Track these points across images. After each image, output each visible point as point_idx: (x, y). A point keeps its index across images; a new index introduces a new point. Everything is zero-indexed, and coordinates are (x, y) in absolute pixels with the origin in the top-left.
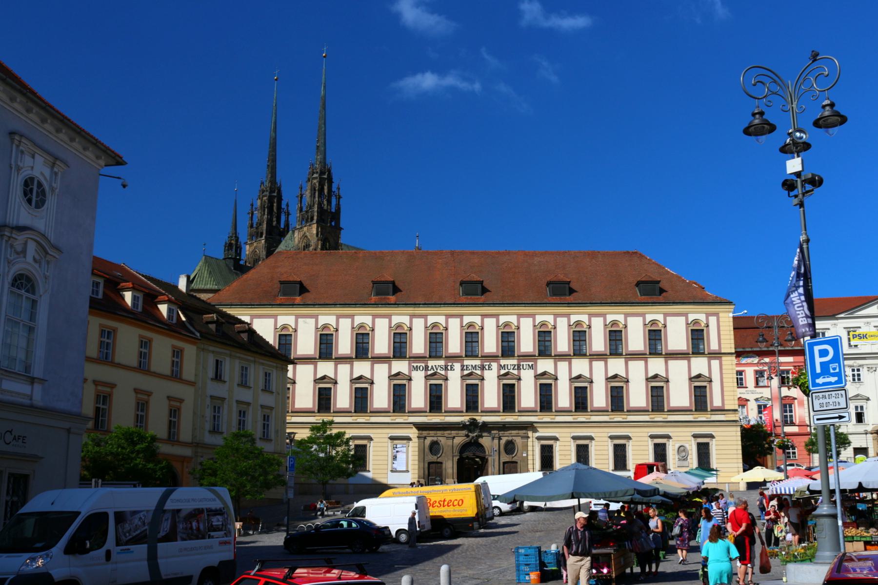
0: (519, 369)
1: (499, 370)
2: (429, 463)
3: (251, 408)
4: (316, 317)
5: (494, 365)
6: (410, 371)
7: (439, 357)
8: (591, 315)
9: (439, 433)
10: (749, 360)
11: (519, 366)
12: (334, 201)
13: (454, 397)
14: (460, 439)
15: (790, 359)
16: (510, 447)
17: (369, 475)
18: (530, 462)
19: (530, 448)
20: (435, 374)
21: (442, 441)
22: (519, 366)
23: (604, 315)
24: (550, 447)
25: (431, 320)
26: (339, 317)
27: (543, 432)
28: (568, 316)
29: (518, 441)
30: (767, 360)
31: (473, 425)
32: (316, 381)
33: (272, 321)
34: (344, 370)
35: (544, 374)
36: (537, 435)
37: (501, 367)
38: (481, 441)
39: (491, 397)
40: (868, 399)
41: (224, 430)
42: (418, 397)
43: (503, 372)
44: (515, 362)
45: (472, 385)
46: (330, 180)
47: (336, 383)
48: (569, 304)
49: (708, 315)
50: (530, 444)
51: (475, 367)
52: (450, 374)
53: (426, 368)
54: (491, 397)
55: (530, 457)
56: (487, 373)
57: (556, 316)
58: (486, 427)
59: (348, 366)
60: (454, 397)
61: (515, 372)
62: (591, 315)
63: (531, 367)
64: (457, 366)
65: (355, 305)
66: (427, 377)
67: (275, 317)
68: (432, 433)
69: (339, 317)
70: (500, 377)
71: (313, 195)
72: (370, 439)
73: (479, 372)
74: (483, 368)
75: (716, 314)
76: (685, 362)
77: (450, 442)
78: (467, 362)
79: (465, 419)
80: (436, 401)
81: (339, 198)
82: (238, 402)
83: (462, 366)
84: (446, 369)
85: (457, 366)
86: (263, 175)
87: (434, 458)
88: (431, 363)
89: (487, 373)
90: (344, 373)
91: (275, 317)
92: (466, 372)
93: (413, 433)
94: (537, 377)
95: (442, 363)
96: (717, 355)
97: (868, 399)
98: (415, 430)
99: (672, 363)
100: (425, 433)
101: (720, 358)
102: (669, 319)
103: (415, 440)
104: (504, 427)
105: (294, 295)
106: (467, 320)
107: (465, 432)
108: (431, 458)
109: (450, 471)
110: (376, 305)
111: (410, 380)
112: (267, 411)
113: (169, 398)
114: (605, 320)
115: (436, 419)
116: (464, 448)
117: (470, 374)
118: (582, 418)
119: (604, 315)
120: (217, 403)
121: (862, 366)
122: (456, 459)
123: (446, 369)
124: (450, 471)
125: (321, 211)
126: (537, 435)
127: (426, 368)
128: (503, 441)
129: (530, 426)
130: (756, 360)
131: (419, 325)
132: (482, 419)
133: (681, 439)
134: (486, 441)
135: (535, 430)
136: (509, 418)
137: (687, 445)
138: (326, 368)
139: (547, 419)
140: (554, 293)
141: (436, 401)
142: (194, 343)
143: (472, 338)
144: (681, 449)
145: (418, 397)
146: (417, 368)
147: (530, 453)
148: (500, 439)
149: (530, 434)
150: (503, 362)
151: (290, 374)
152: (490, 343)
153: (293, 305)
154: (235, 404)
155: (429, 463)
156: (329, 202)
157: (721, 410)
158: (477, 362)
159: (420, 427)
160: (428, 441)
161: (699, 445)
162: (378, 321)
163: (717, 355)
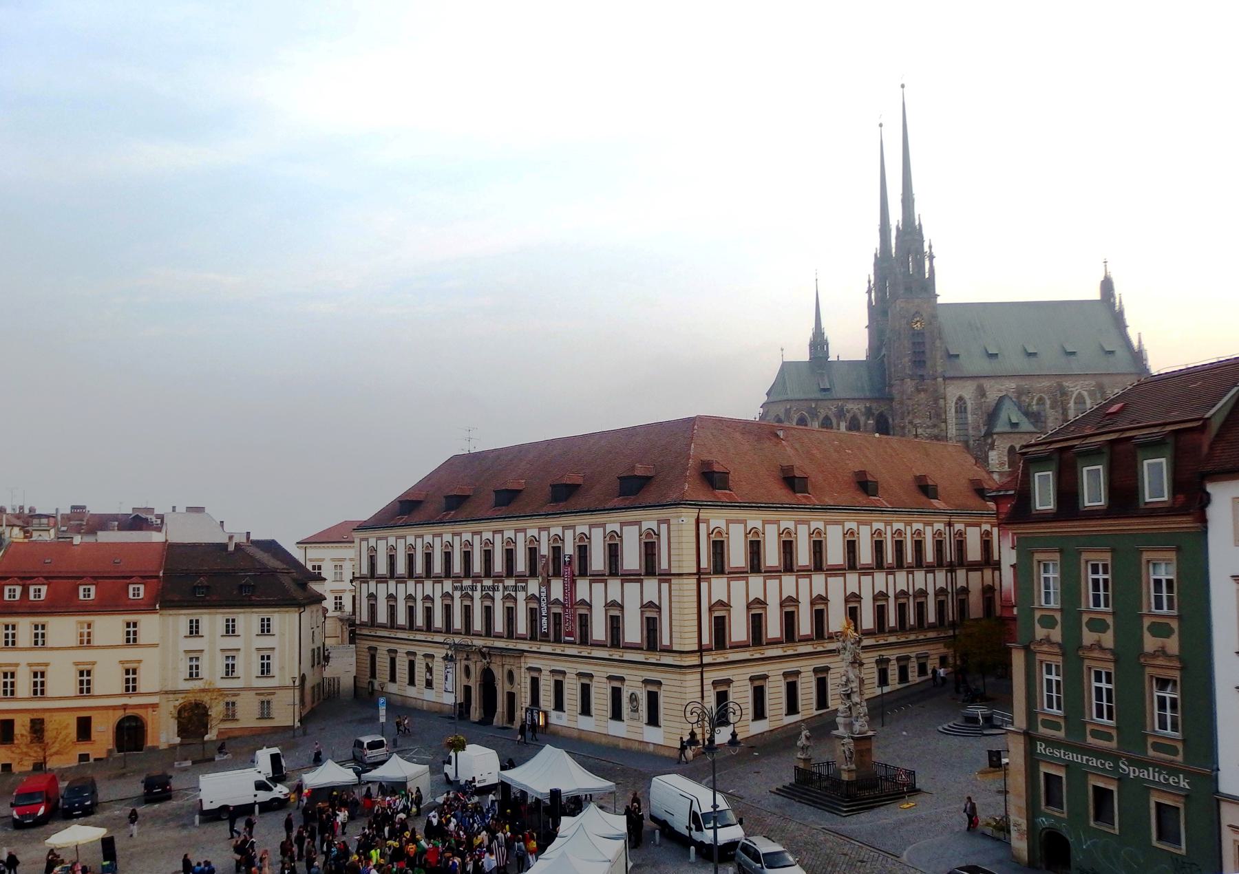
37: (505, 588)
49: (660, 522)
64: (479, 585)
75: (667, 521)
76: (638, 585)
81: (931, 257)
96: (667, 577)
99: (626, 585)
101: (669, 581)
102: (625, 528)
112: (265, 653)
133: (634, 685)
136: (511, 645)
137: (638, 693)
144: (633, 698)
157: (669, 650)
161: (649, 693)
163: (667, 577)
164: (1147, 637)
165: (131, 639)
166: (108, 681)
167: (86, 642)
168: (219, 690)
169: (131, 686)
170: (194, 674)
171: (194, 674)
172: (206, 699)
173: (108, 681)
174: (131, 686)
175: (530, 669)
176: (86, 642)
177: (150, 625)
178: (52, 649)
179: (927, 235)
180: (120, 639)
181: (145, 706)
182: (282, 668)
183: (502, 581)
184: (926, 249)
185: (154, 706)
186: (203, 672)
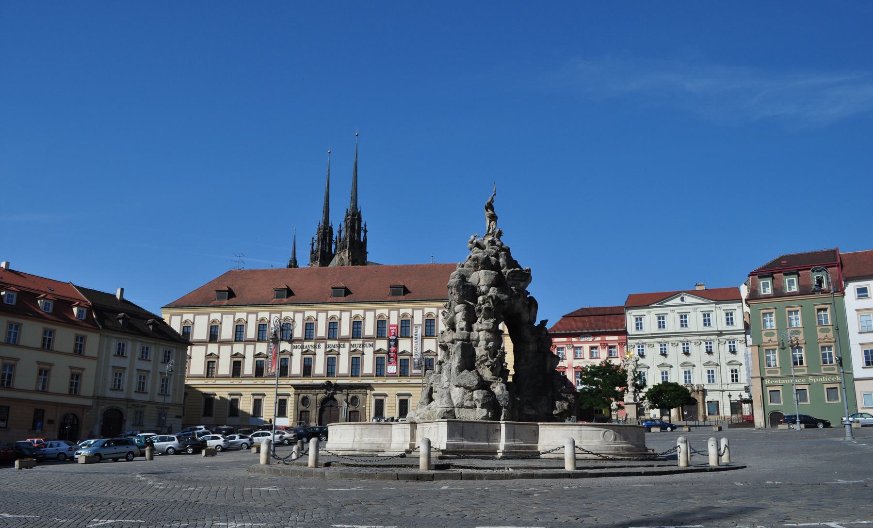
0: (363, 347)
1: (350, 348)
2: (301, 412)
3: (150, 375)
4: (234, 314)
5: (347, 345)
6: (292, 349)
7: (310, 339)
8: (413, 309)
9: (308, 391)
10: (586, 339)
11: (363, 345)
12: (362, 234)
13: (319, 367)
14: (321, 395)
15: (616, 338)
16: (354, 401)
17: (263, 419)
18: (367, 411)
19: (368, 402)
20: (307, 351)
21: (310, 396)
22: (363, 345)
23: (423, 309)
24: (382, 401)
25: (307, 314)
26: (248, 313)
27: (378, 391)
28: (398, 309)
29: (360, 396)
30: (599, 339)
31: (328, 386)
32: (233, 356)
33: (207, 317)
34: (250, 348)
35: (380, 350)
36: (373, 392)
37: (351, 346)
38: (336, 396)
39: (343, 366)
40: (671, 367)
41: (149, 390)
42: (296, 367)
43: (352, 349)
44: (360, 342)
45: (429, 360)
46: (360, 220)
47: (244, 357)
48: (399, 302)
50: (368, 398)
51: (334, 346)
52: (318, 351)
53: (302, 347)
54: (343, 366)
55: (368, 408)
56: (342, 350)
57: (390, 310)
58: (338, 387)
59: (252, 346)
60: (319, 367)
61: (361, 349)
62: (413, 309)
63: (371, 346)
64: (323, 345)
65: (259, 305)
66: (303, 353)
67: (209, 314)
68: (303, 391)
69: (248, 313)
70: (351, 353)
71: (347, 231)
72: (264, 395)
73: (336, 349)
74: (339, 346)
77: (315, 397)
78: (329, 343)
79: (324, 382)
80: (307, 370)
81: (365, 231)
82: (138, 370)
83: (326, 345)
84: (315, 347)
85: (323, 345)
86: (321, 218)
87: (304, 408)
88: (306, 344)
89: (342, 350)
90: (250, 352)
91: (209, 314)
92: (328, 350)
93: (291, 391)
94: (376, 352)
95: (312, 343)
97: (671, 367)
98: (293, 389)
100: (299, 391)
103: (293, 396)
104: (350, 387)
105: (224, 299)
106: (379, 312)
107: (324, 390)
108: (302, 408)
109: (314, 417)
110: (272, 305)
111: (292, 355)
113: (70, 367)
114: (423, 312)
115: (307, 381)
116: (324, 401)
117: (331, 351)
118: (404, 381)
119: (423, 309)
120: (119, 372)
121: (668, 342)
122: (318, 409)
123: (315, 347)
124: (314, 417)
125: (352, 240)
126: (373, 392)
127: (302, 347)
128: (350, 397)
129: (369, 387)
130: (591, 339)
131: (322, 318)
132: (333, 381)
134: (339, 397)
135: (372, 389)
136: (355, 381)
138: (238, 348)
139: (380, 382)
140: (394, 293)
141: (307, 370)
142: (97, 333)
143: (333, 327)
145: (296, 367)
146: (296, 347)
147: (368, 405)
148: (348, 395)
149: (368, 392)
150: (353, 342)
151: (188, 353)
152: (345, 330)
153: (220, 306)
154: (135, 372)
155: (301, 412)
156: (359, 235)
158: (336, 343)
159: (296, 387)
160: (301, 397)
162: (273, 316)
164: (819, 333)
165: (79, 351)
166: (59, 382)
167: (47, 344)
168: (133, 401)
169: (74, 389)
170: (117, 388)
171: (117, 388)
172: (123, 407)
173: (59, 382)
174: (74, 389)
175: (375, 395)
176: (47, 344)
177: (93, 341)
178: (23, 347)
179: (364, 220)
180: (70, 348)
181: (83, 407)
182: (175, 390)
183: (350, 342)
184: (363, 226)
185: (88, 408)
186: (124, 386)
